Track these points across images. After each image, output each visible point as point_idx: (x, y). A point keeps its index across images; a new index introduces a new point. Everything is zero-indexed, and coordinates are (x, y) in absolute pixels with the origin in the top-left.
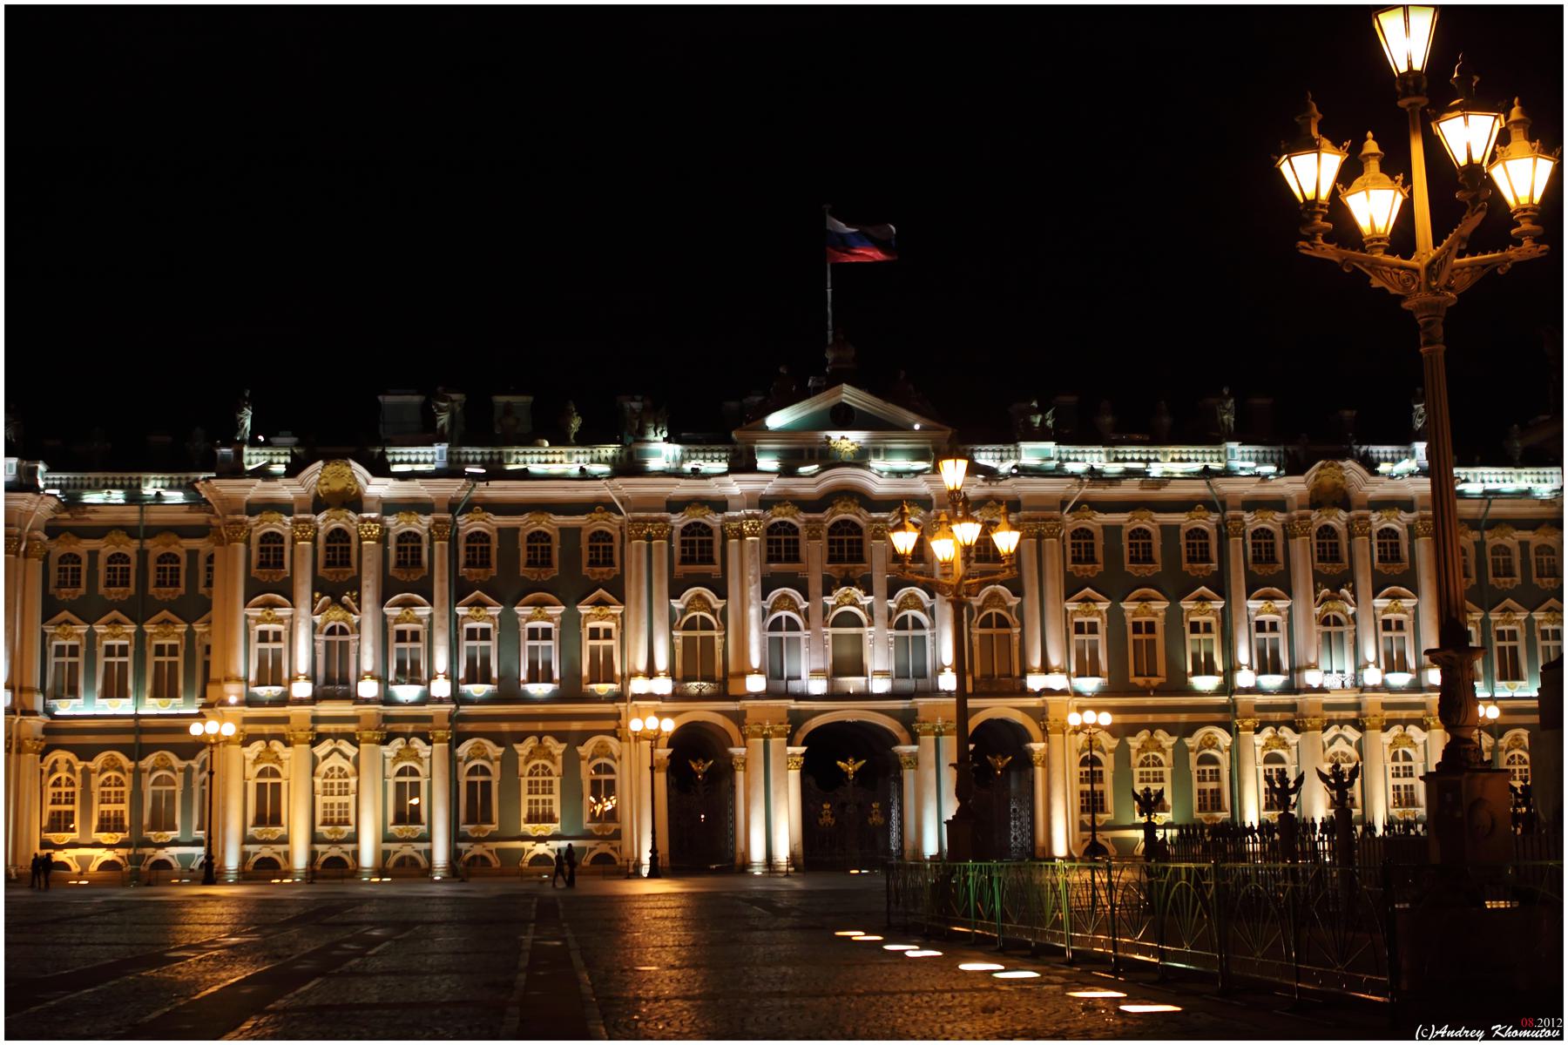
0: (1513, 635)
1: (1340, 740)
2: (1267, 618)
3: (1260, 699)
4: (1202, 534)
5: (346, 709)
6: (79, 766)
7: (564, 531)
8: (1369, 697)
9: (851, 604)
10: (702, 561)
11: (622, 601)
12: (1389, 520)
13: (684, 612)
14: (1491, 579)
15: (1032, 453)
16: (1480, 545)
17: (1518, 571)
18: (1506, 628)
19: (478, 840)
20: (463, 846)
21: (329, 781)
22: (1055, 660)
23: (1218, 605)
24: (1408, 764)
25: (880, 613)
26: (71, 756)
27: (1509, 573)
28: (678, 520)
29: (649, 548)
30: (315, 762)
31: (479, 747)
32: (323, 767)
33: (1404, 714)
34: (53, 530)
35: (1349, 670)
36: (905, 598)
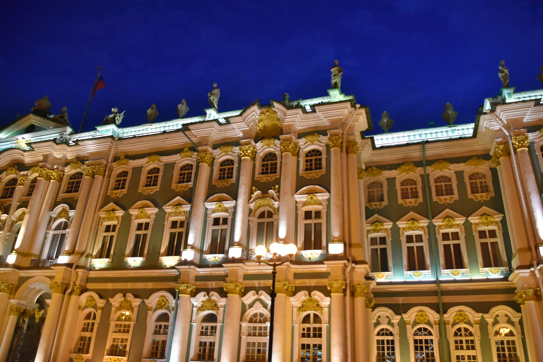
0: (455, 236)
1: (258, 303)
2: (221, 215)
3: (202, 271)
12: (313, 143)
14: (435, 198)
16: (425, 178)
17: (455, 190)
18: (450, 231)
24: (317, 325)
27: (450, 192)
33: (313, 282)
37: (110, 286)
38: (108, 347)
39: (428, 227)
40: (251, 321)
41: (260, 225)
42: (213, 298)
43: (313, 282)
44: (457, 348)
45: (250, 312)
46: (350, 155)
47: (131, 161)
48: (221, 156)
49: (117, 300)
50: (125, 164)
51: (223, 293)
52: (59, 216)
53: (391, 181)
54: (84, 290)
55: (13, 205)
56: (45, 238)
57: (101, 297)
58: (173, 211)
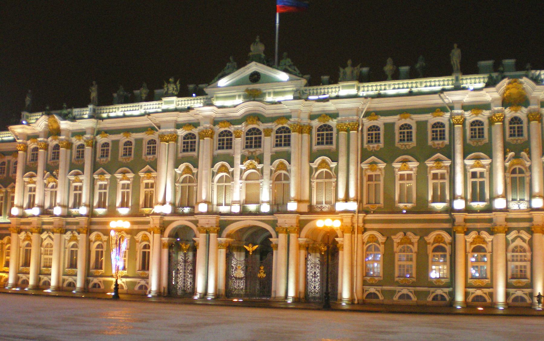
2: (478, 170)
4: (442, 125)
5: (50, 219)
8: (535, 214)
9: (253, 169)
10: (191, 150)
11: (156, 170)
13: (181, 175)
15: (344, 89)
19: (96, 276)
20: (91, 278)
21: (46, 249)
22: (352, 194)
23: (448, 163)
25: (267, 172)
28: (181, 133)
29: (169, 145)
30: (42, 240)
31: (98, 236)
32: (45, 243)
35: (527, 198)
36: (278, 165)
40: (513, 251)
42: (483, 236)
45: (512, 246)
47: (382, 118)
48: (470, 117)
50: (376, 120)
51: (491, 232)
52: (321, 165)
54: (365, 230)
55: (265, 156)
58: (435, 165)
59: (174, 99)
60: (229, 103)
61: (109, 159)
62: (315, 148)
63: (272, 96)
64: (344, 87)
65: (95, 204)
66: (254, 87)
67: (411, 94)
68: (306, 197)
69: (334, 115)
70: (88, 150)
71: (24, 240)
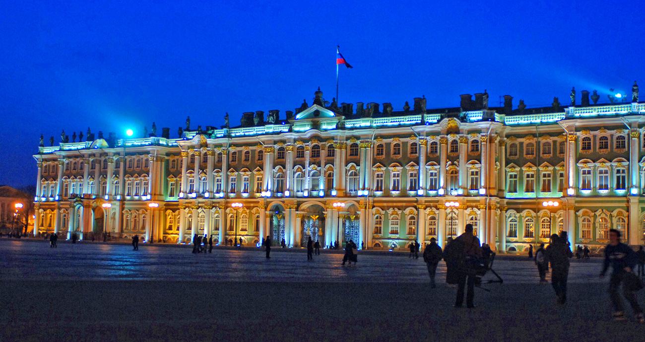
5: (204, 200)
6: (173, 214)
7: (252, 150)
18: (546, 173)
25: (322, 172)
26: (171, 211)
30: (199, 213)
32: (200, 215)
33: (474, 204)
34: (168, 154)
36: (328, 168)
37: (385, 204)
38: (390, 231)
39: (536, 170)
41: (452, 177)
42: (433, 210)
43: (474, 204)
44: (542, 228)
46: (492, 144)
49: (390, 211)
53: (521, 144)
54: (374, 207)
55: (322, 162)
56: (346, 181)
57: (383, 210)
59: (272, 126)
60: (302, 129)
61: (237, 162)
62: (349, 157)
63: (326, 125)
64: (363, 121)
65: (229, 191)
66: (315, 120)
67: (400, 126)
68: (343, 187)
69: (358, 138)
70: (224, 157)
71: (188, 213)
